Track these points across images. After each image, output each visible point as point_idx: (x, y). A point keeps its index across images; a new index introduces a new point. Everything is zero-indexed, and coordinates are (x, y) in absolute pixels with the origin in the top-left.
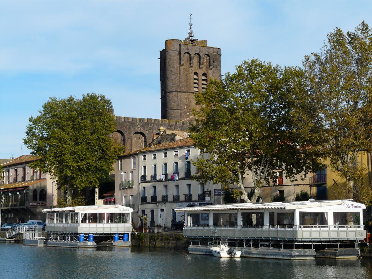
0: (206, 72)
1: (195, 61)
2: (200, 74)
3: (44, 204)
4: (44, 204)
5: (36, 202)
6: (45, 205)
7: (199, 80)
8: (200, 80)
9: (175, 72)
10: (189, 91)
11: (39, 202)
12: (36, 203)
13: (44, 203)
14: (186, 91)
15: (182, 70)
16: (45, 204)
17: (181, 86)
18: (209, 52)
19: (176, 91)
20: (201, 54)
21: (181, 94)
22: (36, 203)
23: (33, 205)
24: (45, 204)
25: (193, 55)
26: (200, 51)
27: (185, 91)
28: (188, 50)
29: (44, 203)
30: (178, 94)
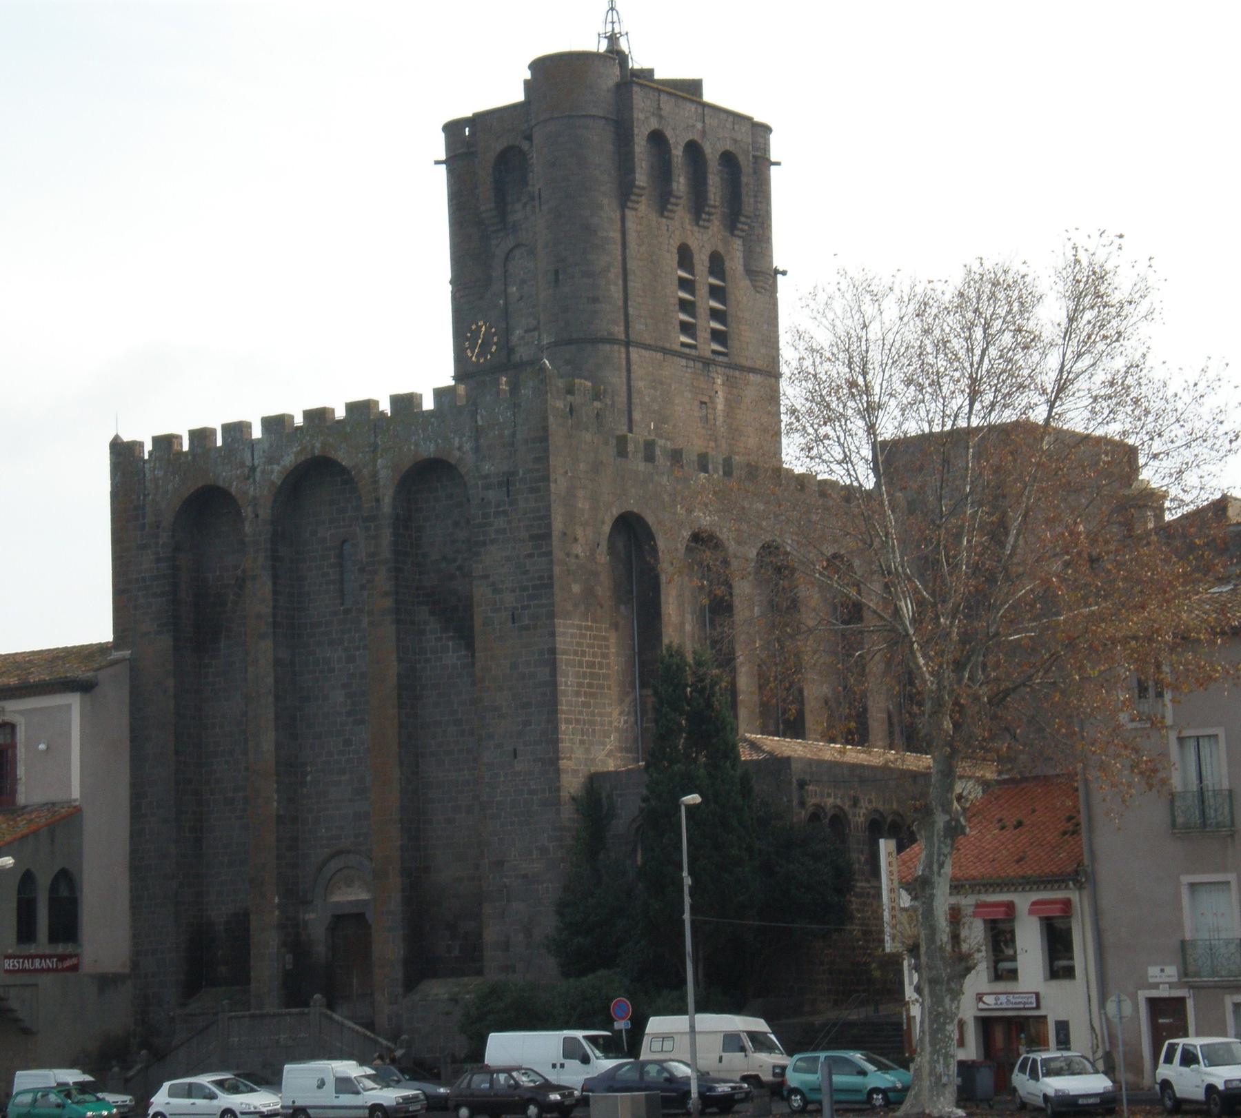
0: (721, 250)
1: (680, 184)
2: (701, 260)
3: (68, 963)
4: (68, 963)
5: (33, 951)
6: (75, 968)
7: (698, 286)
8: (703, 291)
9: (605, 234)
10: (660, 344)
11: (47, 952)
12: (33, 957)
13: (71, 956)
14: (652, 343)
15: (631, 225)
16: (74, 961)
17: (631, 311)
18: (735, 141)
19: (612, 341)
20: (708, 149)
21: (635, 354)
22: (33, 957)
23: (19, 971)
24: (74, 961)
25: (678, 152)
26: (704, 133)
27: (649, 341)
28: (661, 117)
29: (71, 956)
30: (619, 352)
